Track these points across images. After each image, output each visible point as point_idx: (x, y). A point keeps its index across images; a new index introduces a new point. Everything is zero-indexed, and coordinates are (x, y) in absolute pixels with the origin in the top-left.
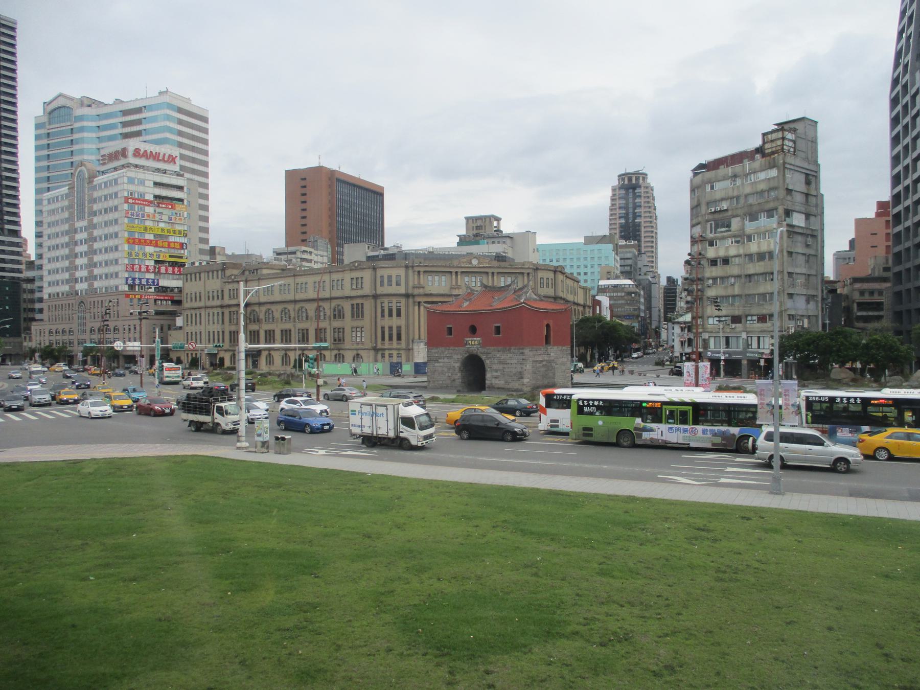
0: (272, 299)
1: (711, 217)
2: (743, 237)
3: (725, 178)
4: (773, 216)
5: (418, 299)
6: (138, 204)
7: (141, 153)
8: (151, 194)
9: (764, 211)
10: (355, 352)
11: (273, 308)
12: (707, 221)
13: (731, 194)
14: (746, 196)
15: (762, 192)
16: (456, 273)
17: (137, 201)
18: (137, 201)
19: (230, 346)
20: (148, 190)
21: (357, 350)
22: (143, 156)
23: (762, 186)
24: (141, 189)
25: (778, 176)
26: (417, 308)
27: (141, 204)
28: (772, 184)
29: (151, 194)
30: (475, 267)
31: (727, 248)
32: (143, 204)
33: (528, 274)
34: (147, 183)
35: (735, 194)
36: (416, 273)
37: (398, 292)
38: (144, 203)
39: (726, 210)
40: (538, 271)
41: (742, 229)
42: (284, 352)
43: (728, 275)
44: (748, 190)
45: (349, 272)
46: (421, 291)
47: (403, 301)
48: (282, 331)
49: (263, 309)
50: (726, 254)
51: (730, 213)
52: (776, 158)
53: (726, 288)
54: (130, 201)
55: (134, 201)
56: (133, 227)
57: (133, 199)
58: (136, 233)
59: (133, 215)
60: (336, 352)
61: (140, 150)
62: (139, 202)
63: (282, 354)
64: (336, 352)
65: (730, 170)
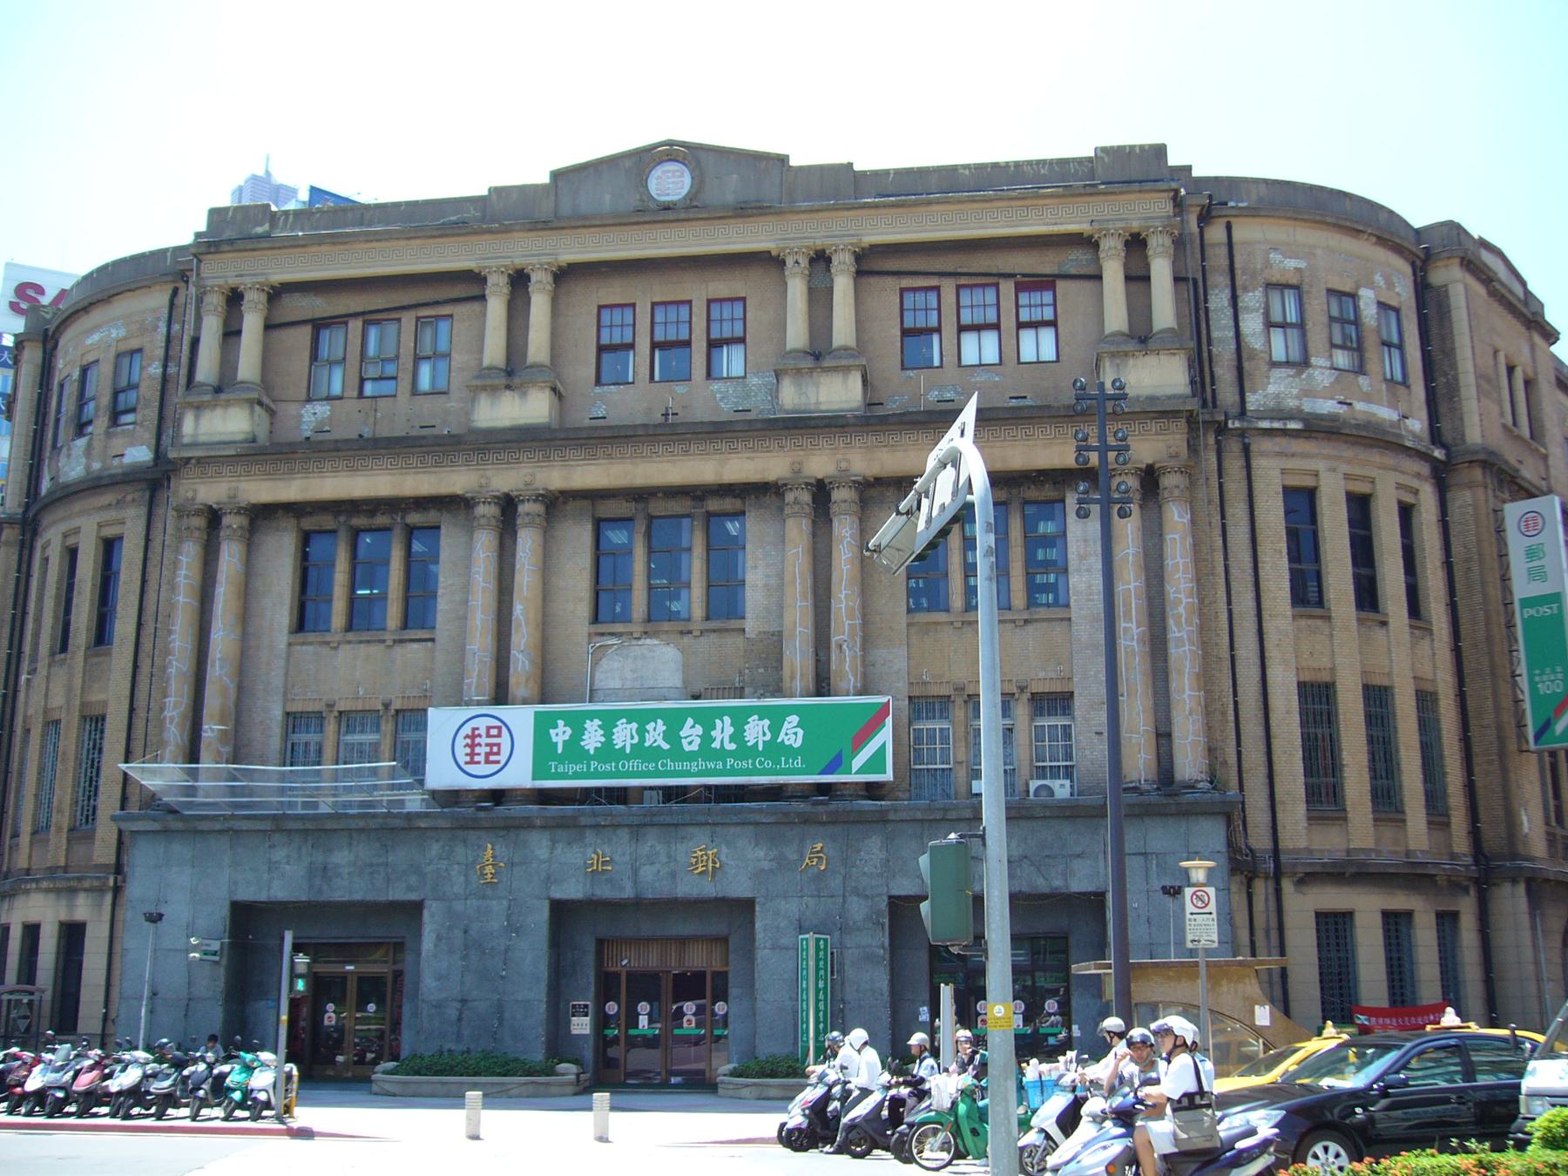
5: (210, 491)
26: (189, 557)
33: (1136, 244)
36: (215, 301)
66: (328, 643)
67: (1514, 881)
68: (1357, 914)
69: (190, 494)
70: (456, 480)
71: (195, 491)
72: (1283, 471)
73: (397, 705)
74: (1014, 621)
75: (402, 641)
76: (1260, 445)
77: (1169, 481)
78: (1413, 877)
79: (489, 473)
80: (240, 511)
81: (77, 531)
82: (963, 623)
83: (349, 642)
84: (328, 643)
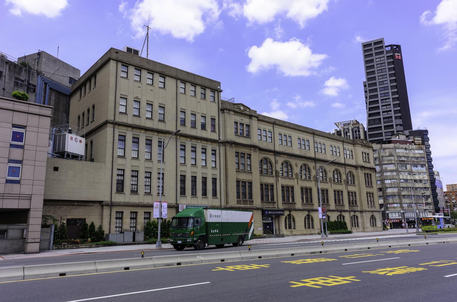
0: (289, 151)
1: (399, 162)
2: (411, 173)
3: (402, 148)
4: (423, 167)
9: (420, 165)
10: (371, 214)
11: (293, 161)
12: (398, 164)
13: (405, 155)
14: (411, 157)
15: (417, 158)
19: (238, 202)
21: (372, 212)
23: (417, 155)
25: (424, 153)
28: (422, 156)
31: (407, 176)
35: (407, 155)
39: (405, 161)
41: (411, 170)
42: (306, 213)
43: (408, 186)
44: (412, 155)
45: (360, 146)
48: (302, 189)
49: (281, 160)
50: (407, 178)
51: (406, 162)
52: (422, 147)
53: (408, 192)
60: (352, 214)
63: (304, 216)
64: (352, 214)
65: (404, 146)
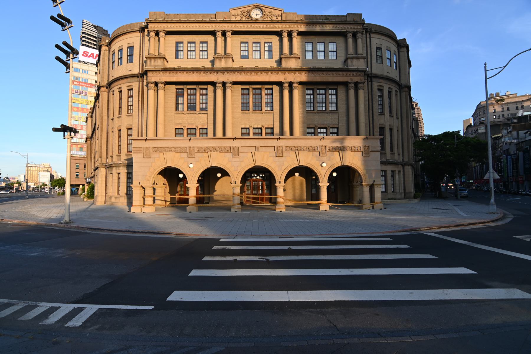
6: (82, 85)
7: (89, 55)
8: (93, 80)
16: (224, 34)
17: (81, 84)
18: (81, 84)
20: (90, 77)
22: (90, 56)
24: (85, 76)
26: (152, 93)
27: (84, 86)
29: (93, 80)
30: (256, 22)
32: (86, 86)
34: (90, 73)
37: (130, 73)
38: (87, 85)
40: (373, 35)
46: (159, 64)
47: (135, 85)
54: (75, 83)
55: (78, 83)
56: (77, 100)
57: (77, 82)
58: (80, 104)
59: (78, 93)
61: (88, 53)
62: (83, 84)
66: (183, 113)
67: (408, 165)
68: (388, 171)
69: (150, 79)
70: (212, 78)
71: (151, 78)
72: (378, 86)
73: (199, 127)
74: (327, 113)
75: (200, 113)
76: (374, 80)
77: (360, 85)
78: (396, 164)
79: (219, 77)
80: (163, 83)
81: (121, 88)
82: (318, 113)
83: (188, 113)
84: (183, 113)
